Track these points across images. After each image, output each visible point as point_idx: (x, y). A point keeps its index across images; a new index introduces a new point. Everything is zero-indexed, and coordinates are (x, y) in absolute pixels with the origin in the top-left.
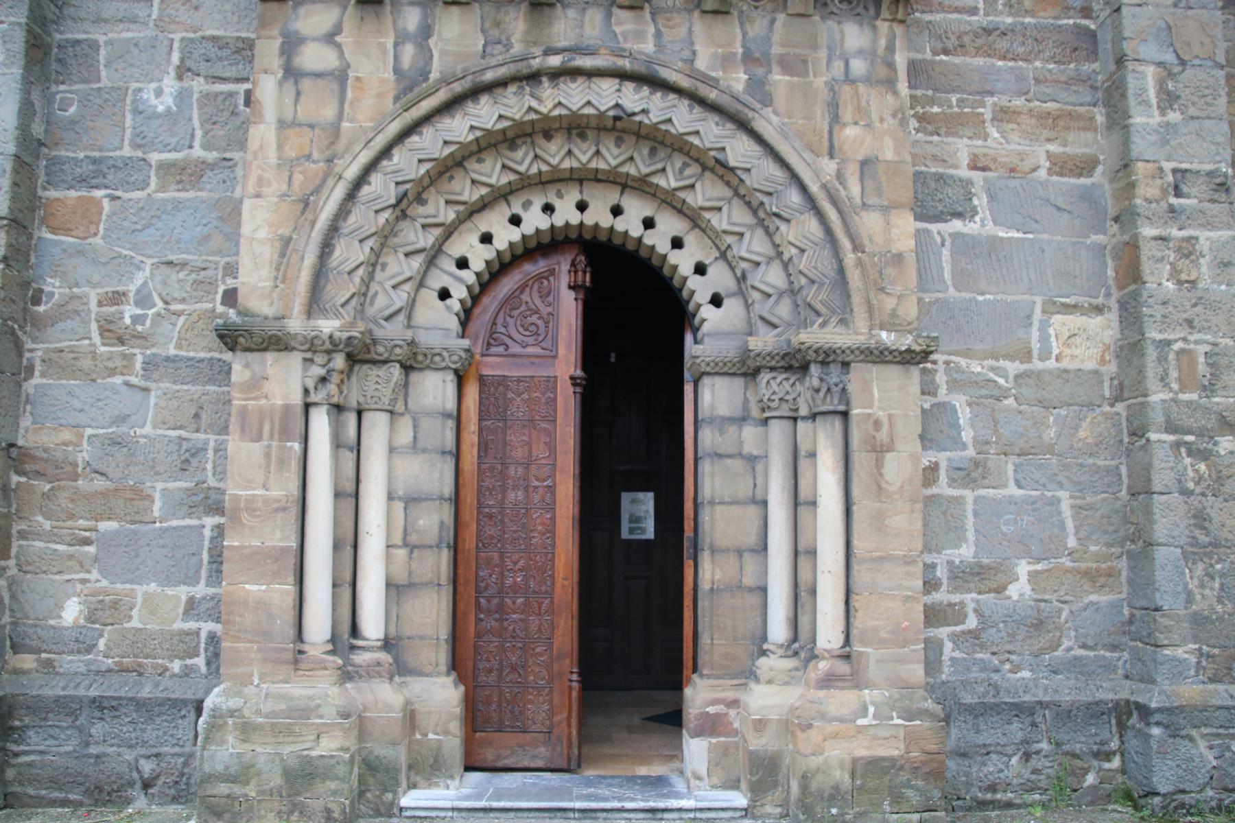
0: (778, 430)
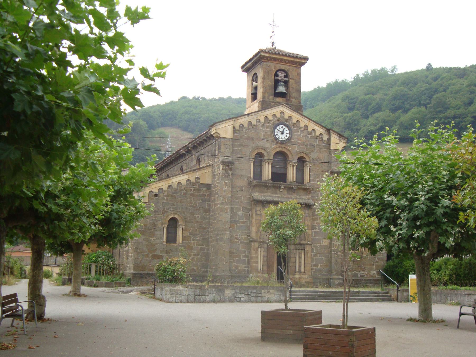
0: (298, 251)
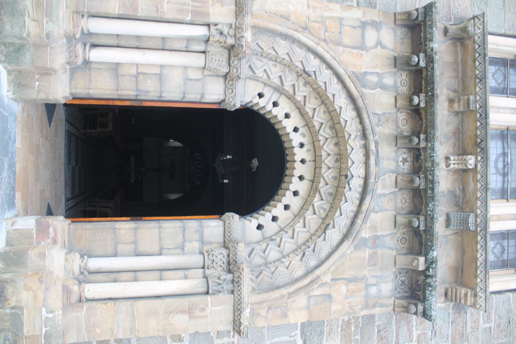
0: (198, 260)
